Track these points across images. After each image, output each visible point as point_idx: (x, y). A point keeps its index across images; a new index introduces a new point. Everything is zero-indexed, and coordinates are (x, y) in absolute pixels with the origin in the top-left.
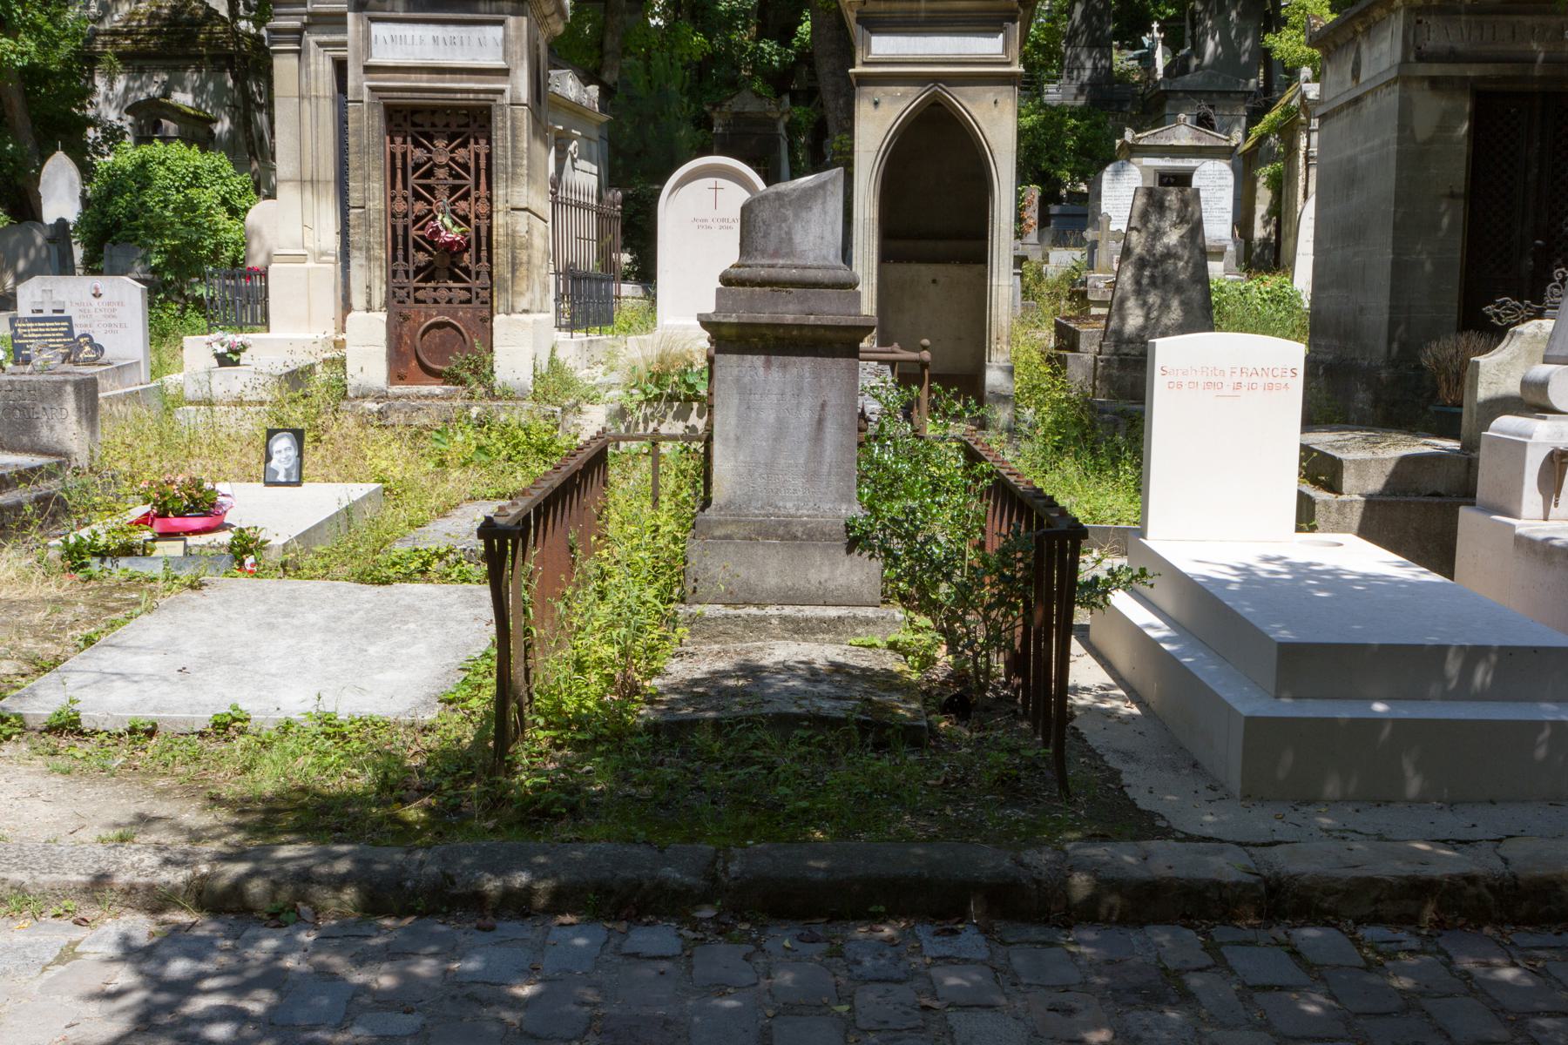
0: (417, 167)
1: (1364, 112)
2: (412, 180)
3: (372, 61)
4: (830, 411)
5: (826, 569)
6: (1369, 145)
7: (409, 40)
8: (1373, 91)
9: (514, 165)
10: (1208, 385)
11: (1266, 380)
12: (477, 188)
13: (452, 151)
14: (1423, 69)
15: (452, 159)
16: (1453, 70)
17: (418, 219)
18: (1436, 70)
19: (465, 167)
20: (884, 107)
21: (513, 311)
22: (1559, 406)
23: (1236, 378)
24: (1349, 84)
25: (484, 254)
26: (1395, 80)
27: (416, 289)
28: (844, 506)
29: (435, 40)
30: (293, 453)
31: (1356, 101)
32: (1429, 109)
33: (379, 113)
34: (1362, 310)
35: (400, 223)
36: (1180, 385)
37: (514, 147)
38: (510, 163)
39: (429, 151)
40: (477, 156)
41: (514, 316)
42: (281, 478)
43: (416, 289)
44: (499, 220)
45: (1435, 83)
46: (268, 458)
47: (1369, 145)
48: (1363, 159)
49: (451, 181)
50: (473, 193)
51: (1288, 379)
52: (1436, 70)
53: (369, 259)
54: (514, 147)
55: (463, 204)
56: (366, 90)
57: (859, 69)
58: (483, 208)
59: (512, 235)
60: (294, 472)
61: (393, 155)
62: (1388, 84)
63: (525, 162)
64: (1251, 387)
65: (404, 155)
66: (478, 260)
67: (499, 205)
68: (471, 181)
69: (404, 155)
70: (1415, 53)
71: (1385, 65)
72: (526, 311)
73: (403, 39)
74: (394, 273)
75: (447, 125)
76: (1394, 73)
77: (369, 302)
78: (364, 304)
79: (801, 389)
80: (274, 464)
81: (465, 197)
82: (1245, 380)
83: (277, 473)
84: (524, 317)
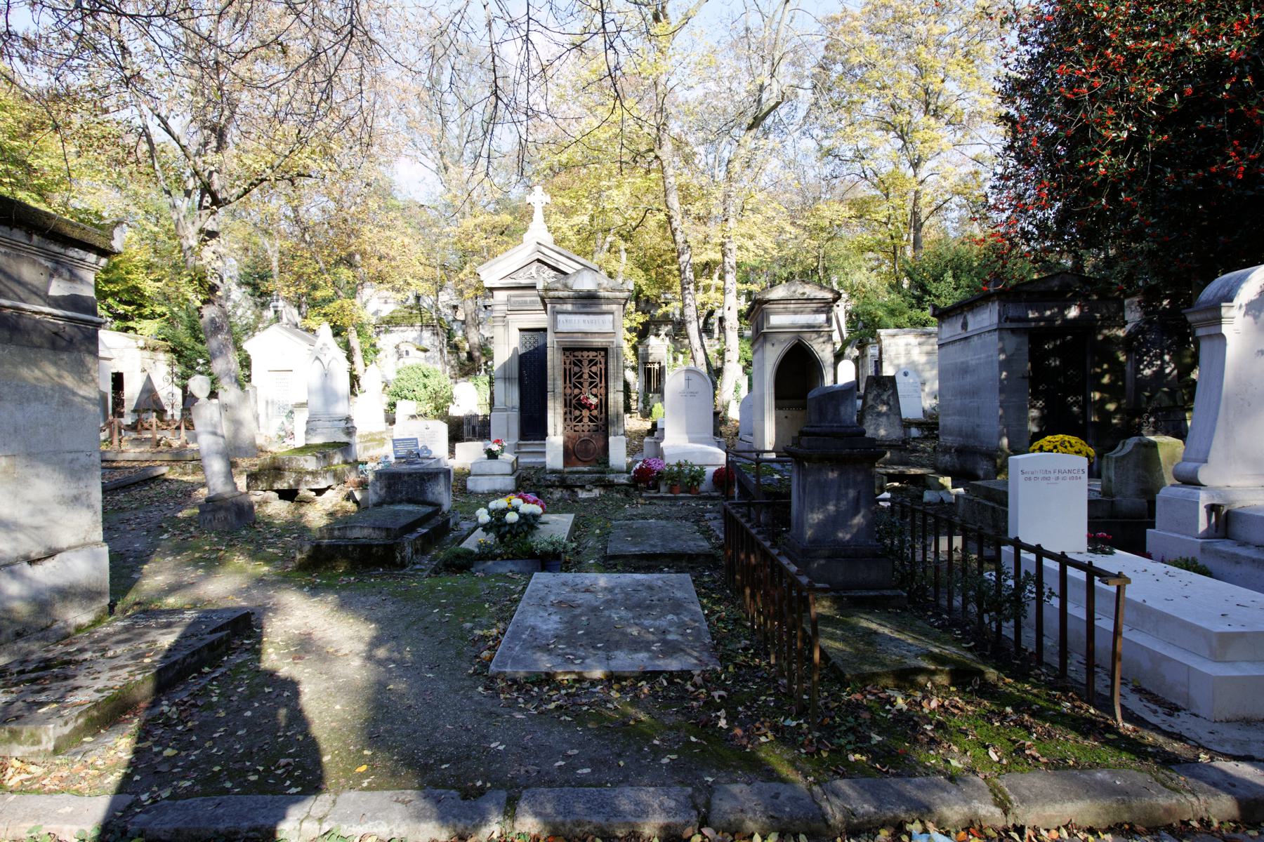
0: (575, 374)
1: (972, 343)
2: (573, 380)
10: (1044, 478)
11: (1070, 475)
14: (1008, 325)
16: (1021, 325)
17: (576, 396)
18: (1014, 325)
19: (596, 374)
20: (776, 346)
22: (1203, 483)
23: (1057, 475)
24: (959, 329)
26: (995, 330)
31: (966, 338)
32: (1012, 342)
33: (561, 351)
34: (978, 426)
35: (568, 398)
36: (1030, 479)
45: (1013, 331)
48: (974, 362)
51: (1081, 474)
52: (1014, 325)
55: (594, 390)
57: (765, 330)
61: (565, 369)
64: (1064, 479)
66: (601, 413)
68: (598, 380)
70: (1003, 317)
71: (986, 323)
73: (571, 321)
74: (565, 420)
76: (995, 327)
81: (596, 386)
82: (1061, 475)
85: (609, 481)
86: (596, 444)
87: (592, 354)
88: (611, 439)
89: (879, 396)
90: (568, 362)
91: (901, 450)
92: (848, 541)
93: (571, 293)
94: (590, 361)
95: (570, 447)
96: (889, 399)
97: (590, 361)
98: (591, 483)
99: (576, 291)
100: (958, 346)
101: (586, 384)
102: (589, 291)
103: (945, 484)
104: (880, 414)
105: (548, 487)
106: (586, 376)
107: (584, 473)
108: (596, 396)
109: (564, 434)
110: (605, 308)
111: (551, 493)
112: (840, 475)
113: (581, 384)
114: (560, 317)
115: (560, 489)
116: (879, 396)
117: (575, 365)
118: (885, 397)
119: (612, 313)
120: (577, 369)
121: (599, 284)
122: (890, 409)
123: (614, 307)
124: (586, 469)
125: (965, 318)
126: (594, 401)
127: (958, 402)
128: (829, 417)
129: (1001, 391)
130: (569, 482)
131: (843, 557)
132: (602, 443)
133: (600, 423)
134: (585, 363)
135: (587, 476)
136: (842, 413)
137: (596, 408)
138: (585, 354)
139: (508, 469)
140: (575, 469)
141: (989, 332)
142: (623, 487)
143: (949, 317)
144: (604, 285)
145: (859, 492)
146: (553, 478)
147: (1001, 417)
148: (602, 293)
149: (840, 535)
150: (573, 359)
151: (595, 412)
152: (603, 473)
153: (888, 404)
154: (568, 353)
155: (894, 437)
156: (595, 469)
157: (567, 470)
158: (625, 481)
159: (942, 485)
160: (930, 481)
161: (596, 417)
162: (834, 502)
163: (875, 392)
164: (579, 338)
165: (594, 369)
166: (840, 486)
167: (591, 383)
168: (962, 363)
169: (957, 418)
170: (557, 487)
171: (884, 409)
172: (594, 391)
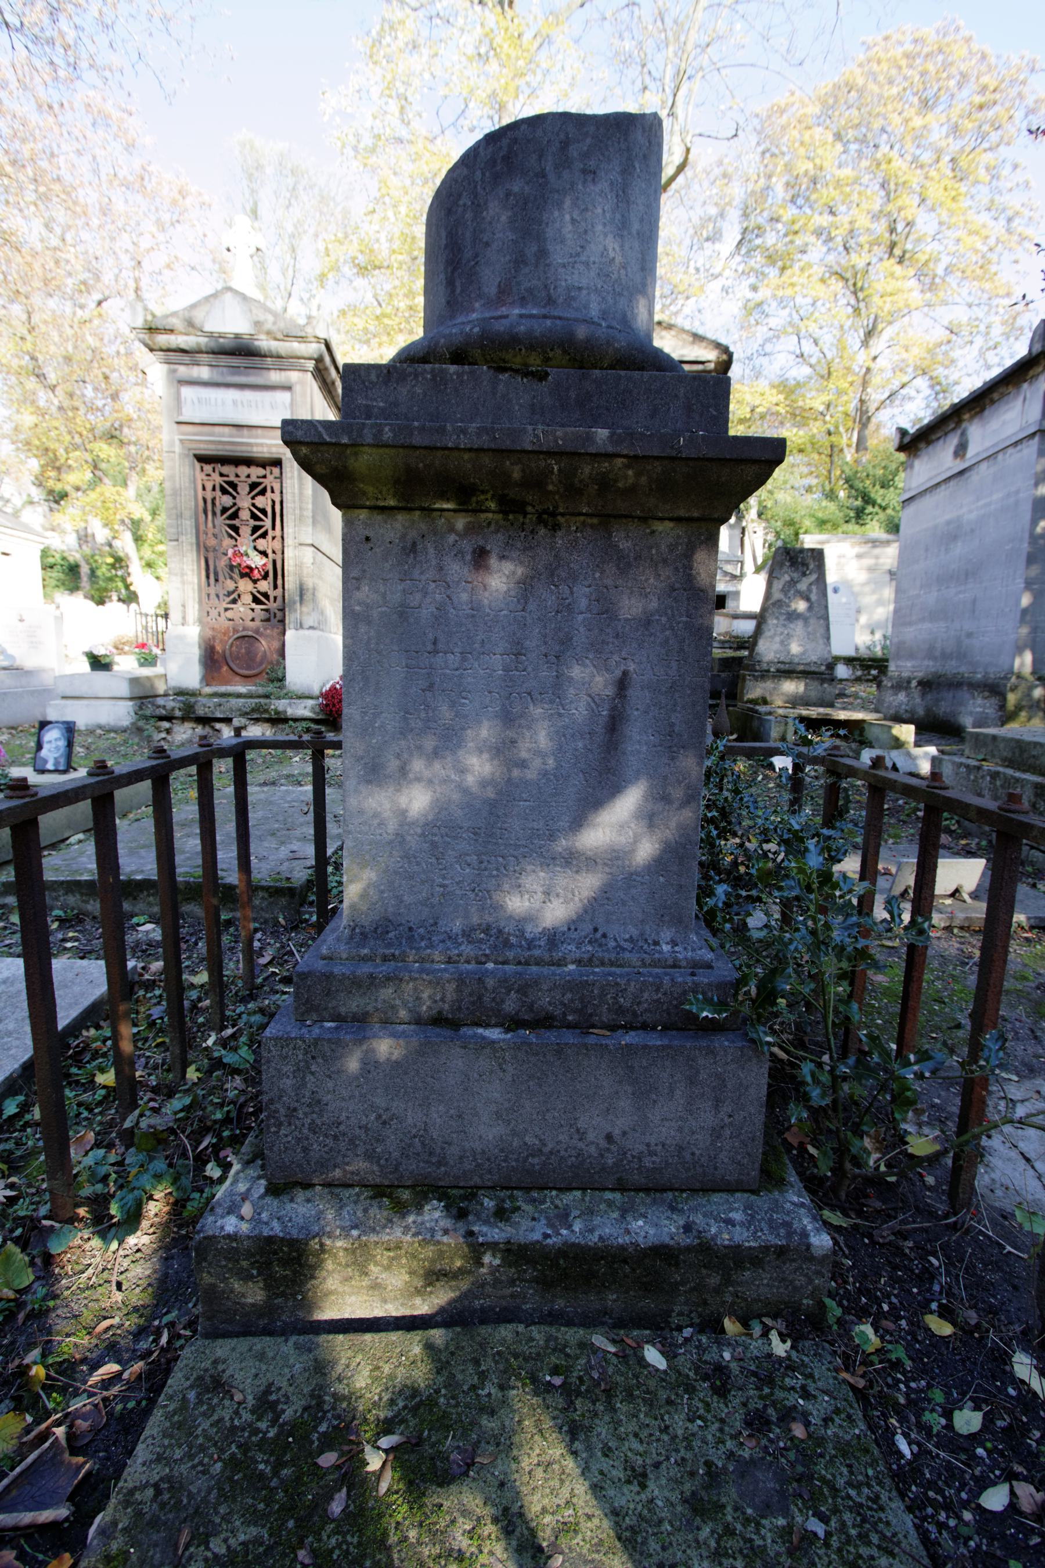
0: (224, 510)
3: (181, 419)
4: (638, 698)
5: (625, 1103)
6: (981, 503)
7: (213, 402)
8: (991, 457)
9: (301, 509)
12: (274, 528)
13: (253, 498)
15: (253, 505)
19: (264, 512)
21: (301, 627)
25: (279, 582)
27: (226, 610)
28: (666, 934)
29: (235, 402)
30: (62, 743)
31: (961, 473)
34: (970, 635)
37: (301, 494)
38: (297, 505)
39: (234, 498)
40: (273, 502)
41: (301, 632)
42: (50, 766)
43: (226, 610)
44: (289, 553)
46: (39, 747)
47: (981, 503)
48: (973, 516)
49: (252, 523)
50: (271, 533)
53: (183, 583)
54: (301, 494)
55: (261, 541)
56: (177, 443)
58: (277, 545)
59: (299, 566)
60: (62, 761)
62: (1034, 434)
63: (310, 506)
65: (214, 500)
66: (275, 587)
67: (289, 541)
69: (214, 500)
72: (311, 628)
75: (248, 476)
77: (184, 618)
78: (180, 620)
79: (566, 642)
80: (44, 753)
81: (264, 535)
83: (46, 761)
84: (311, 632)
85: (277, 712)
86: (265, 645)
87: (256, 472)
88: (290, 635)
89: (793, 582)
90: (209, 486)
91: (823, 681)
92: (553, 938)
93: (203, 341)
94: (253, 486)
95: (219, 648)
96: (809, 590)
97: (253, 486)
98: (244, 714)
99: (211, 335)
100: (943, 492)
101: (245, 531)
102: (237, 336)
103: (903, 738)
104: (793, 616)
105: (162, 718)
106: (245, 515)
107: (239, 696)
108: (264, 554)
109: (200, 621)
110: (275, 377)
111: (168, 731)
112: (526, 588)
113: (236, 529)
114: (187, 392)
115: (188, 725)
116: (793, 582)
117: (224, 491)
118: (803, 586)
119: (288, 388)
120: (227, 500)
121: (257, 324)
122: (810, 608)
123: (294, 376)
124: (242, 689)
125: (963, 434)
126: (256, 561)
127: (931, 598)
128: (490, 279)
129: (1031, 559)
130: (201, 712)
131: (513, 1024)
132: (276, 644)
133: (272, 605)
134: (243, 489)
135: (234, 702)
136: (558, 255)
137: (265, 577)
138: (243, 470)
139: (124, 690)
140: (223, 689)
141: (1016, 444)
142: (304, 724)
143: (929, 443)
144: (268, 326)
145: (622, 684)
146: (170, 703)
147: (1025, 612)
148: (264, 343)
149: (516, 904)
150: (219, 480)
151: (264, 586)
152: (267, 696)
153: (808, 599)
154: (208, 468)
155: (814, 658)
156: (261, 690)
157: (208, 690)
158: (308, 714)
159: (897, 739)
160: (871, 733)
161: (266, 595)
162: (486, 731)
163: (787, 578)
164: (225, 435)
165: (260, 502)
166: (518, 651)
167: (255, 529)
168: (948, 523)
169: (927, 625)
170: (183, 719)
171: (801, 606)
172: (262, 544)
